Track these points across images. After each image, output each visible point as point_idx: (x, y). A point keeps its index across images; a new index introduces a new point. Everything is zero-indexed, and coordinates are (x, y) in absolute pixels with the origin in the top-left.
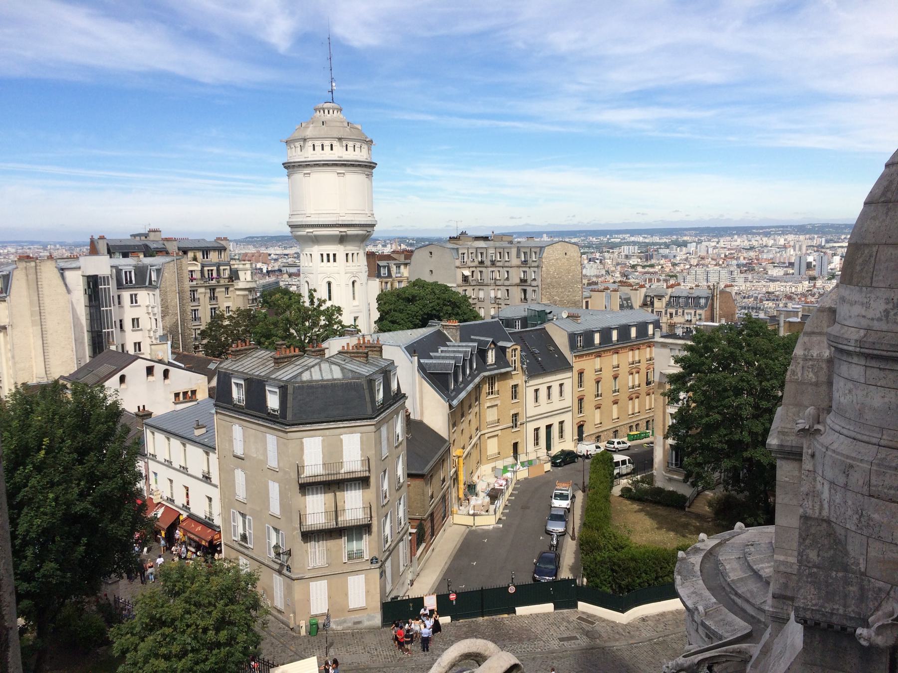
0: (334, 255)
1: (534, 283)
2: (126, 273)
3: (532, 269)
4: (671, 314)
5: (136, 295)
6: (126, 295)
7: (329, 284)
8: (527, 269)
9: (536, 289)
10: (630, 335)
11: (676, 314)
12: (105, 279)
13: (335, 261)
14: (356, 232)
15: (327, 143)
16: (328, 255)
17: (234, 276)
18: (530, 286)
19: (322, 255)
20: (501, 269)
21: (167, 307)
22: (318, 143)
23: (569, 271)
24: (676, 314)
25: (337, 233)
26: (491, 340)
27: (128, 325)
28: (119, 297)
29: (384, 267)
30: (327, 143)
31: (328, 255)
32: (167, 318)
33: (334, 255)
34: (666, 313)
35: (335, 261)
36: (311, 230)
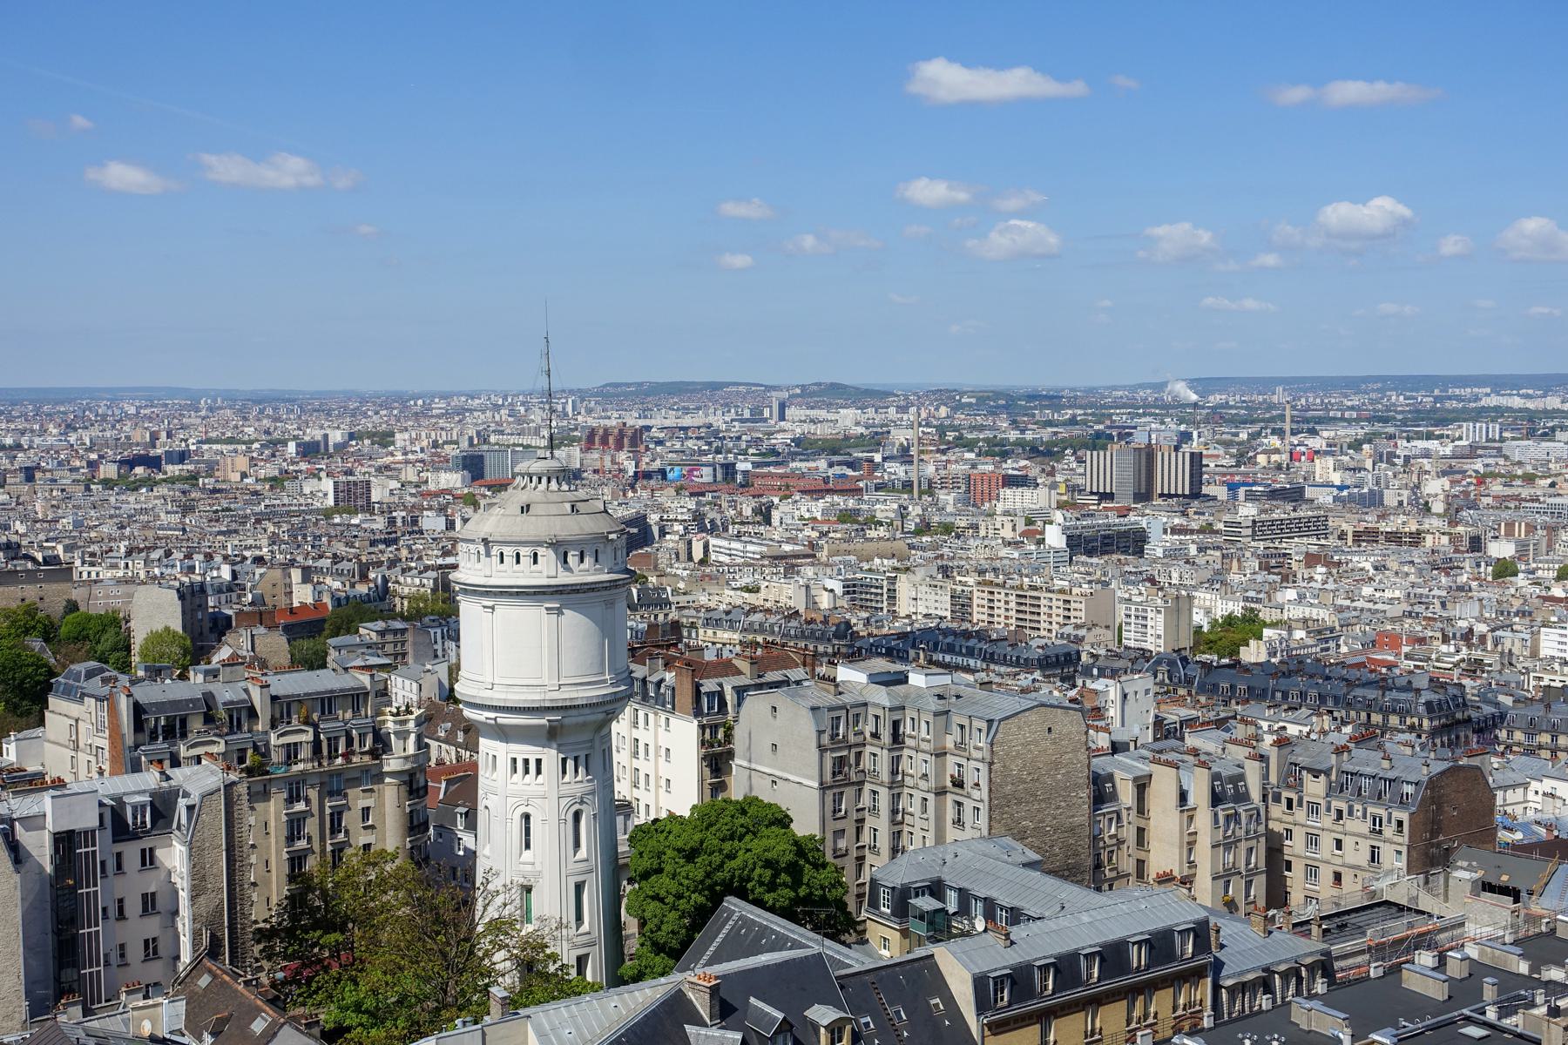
0: (539, 762)
1: (976, 794)
2: (135, 808)
3: (973, 764)
4: (1340, 813)
5: (151, 850)
6: (131, 851)
7: (527, 817)
8: (963, 762)
9: (980, 805)
10: (1128, 961)
11: (1350, 813)
12: (89, 835)
13: (539, 772)
14: (581, 719)
15: (525, 551)
16: (526, 762)
17: (381, 744)
18: (969, 796)
19: (514, 760)
20: (913, 753)
21: (203, 878)
22: (509, 551)
23: (1056, 765)
24: (1350, 813)
25: (544, 722)
26: (780, 1016)
27: (133, 907)
28: (119, 855)
29: (710, 695)
30: (525, 551)
31: (526, 762)
32: (202, 899)
33: (539, 762)
34: (1329, 810)
35: (539, 772)
36: (492, 715)
